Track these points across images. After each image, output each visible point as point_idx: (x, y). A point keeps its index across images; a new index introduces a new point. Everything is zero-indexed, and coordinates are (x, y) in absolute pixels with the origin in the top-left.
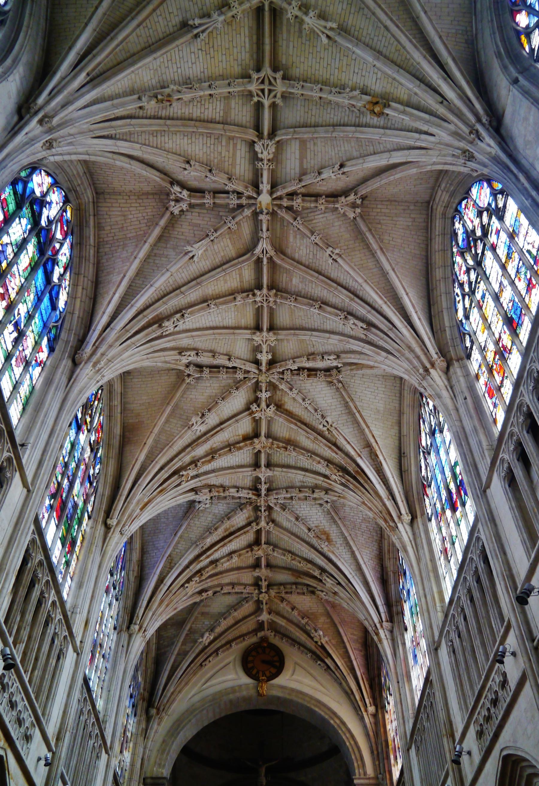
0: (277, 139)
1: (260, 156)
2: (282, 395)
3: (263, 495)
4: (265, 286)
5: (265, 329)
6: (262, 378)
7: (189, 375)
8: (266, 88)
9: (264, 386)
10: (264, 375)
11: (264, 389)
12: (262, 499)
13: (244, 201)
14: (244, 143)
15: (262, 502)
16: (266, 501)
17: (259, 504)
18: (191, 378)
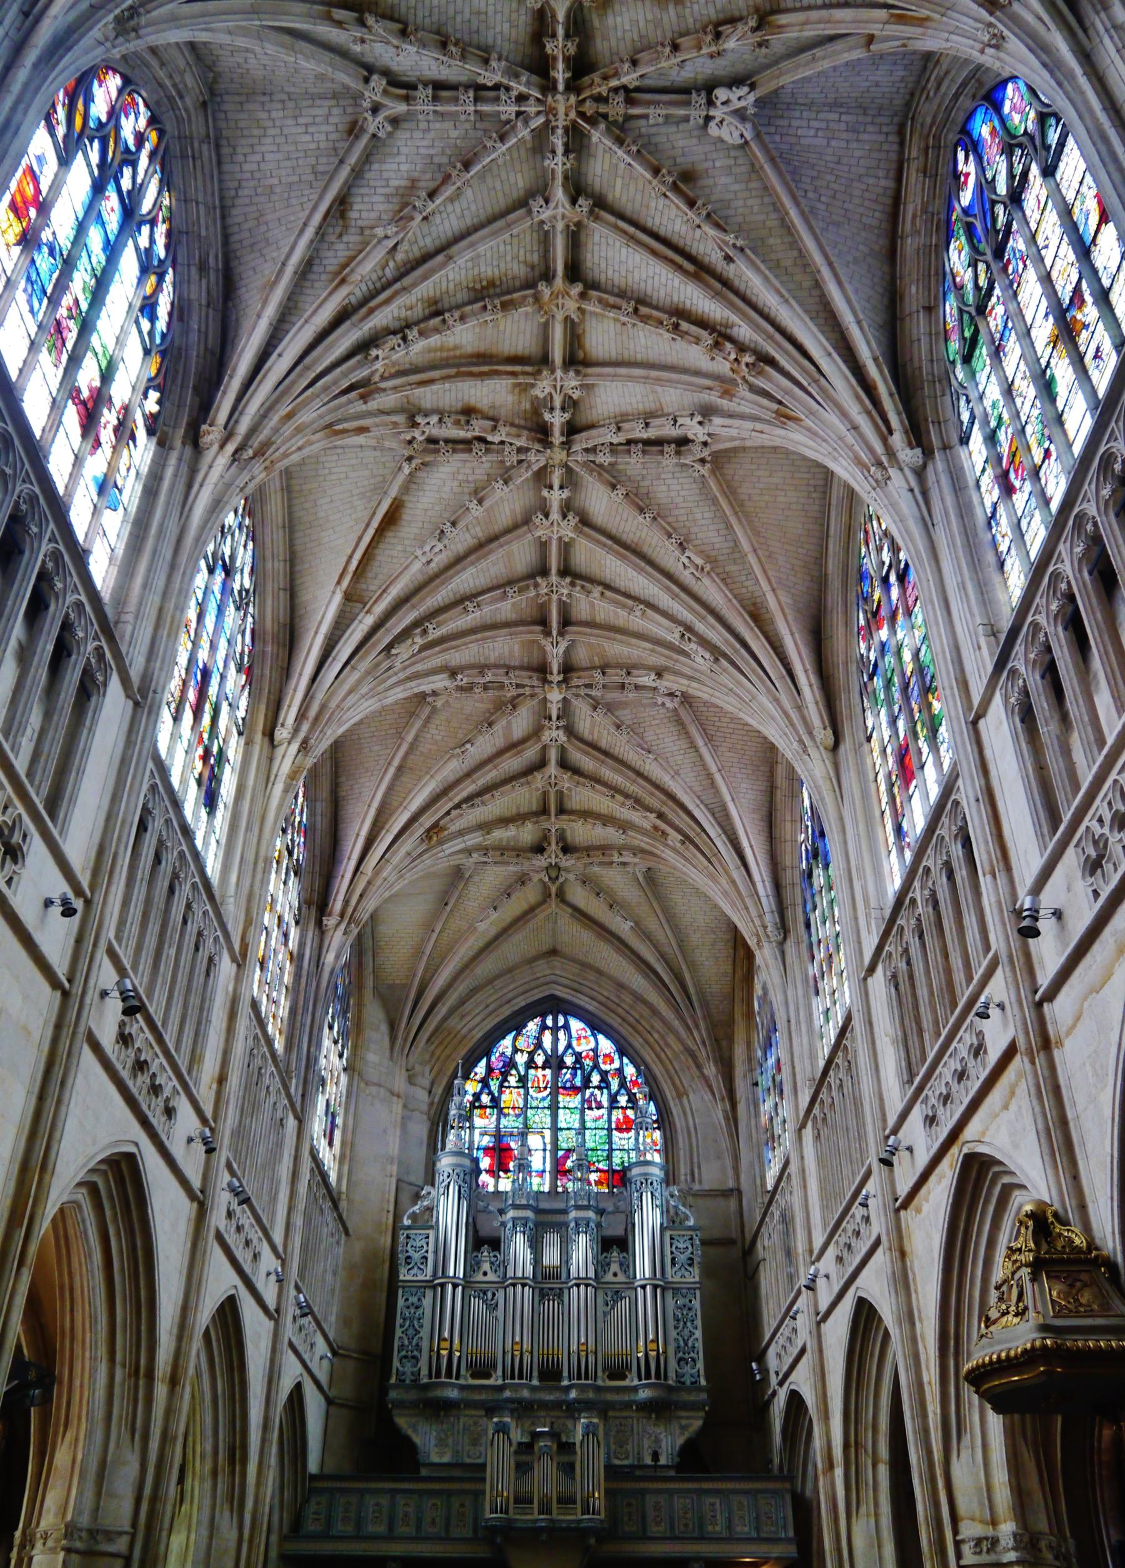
0: (538, 747)
1: (561, 732)
2: (520, 402)
3: (560, 132)
4: (554, 571)
5: (554, 571)
6: (559, 455)
7: (703, 461)
8: (553, 780)
9: (557, 438)
10: (557, 462)
11: (556, 484)
12: (561, 123)
13: (583, 691)
14: (581, 730)
15: (561, 110)
16: (551, 111)
17: (573, 99)
18: (698, 457)
